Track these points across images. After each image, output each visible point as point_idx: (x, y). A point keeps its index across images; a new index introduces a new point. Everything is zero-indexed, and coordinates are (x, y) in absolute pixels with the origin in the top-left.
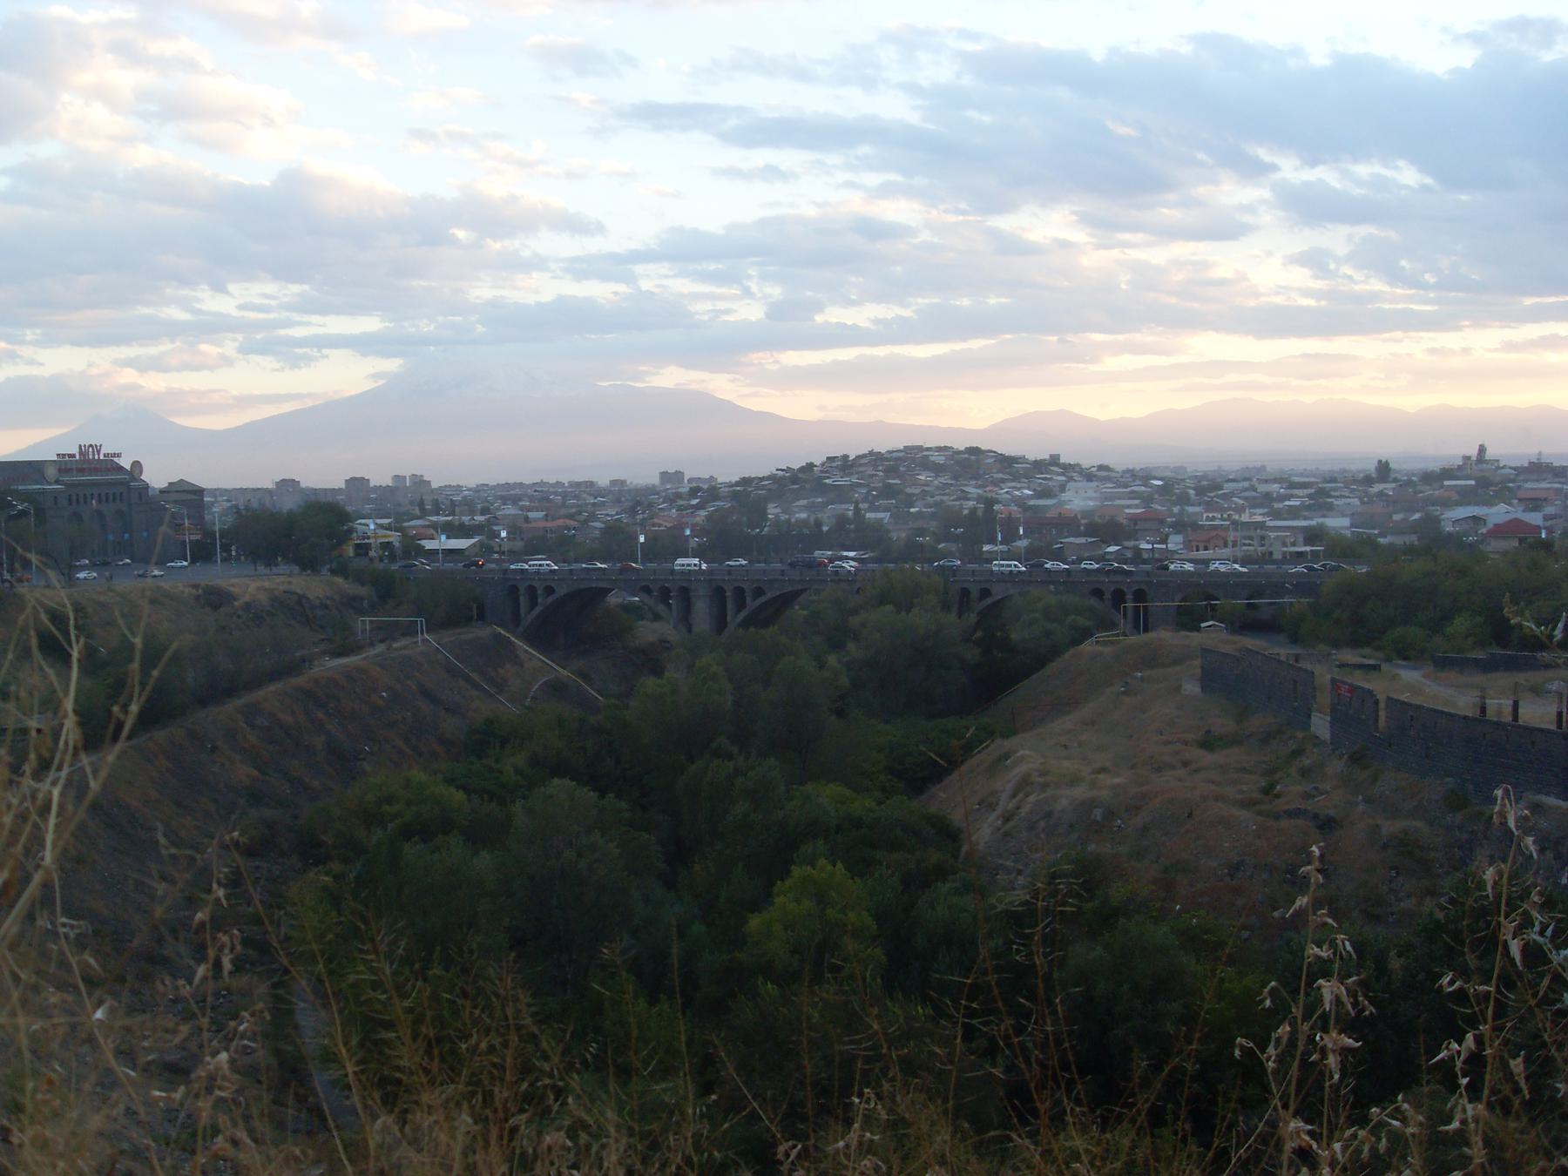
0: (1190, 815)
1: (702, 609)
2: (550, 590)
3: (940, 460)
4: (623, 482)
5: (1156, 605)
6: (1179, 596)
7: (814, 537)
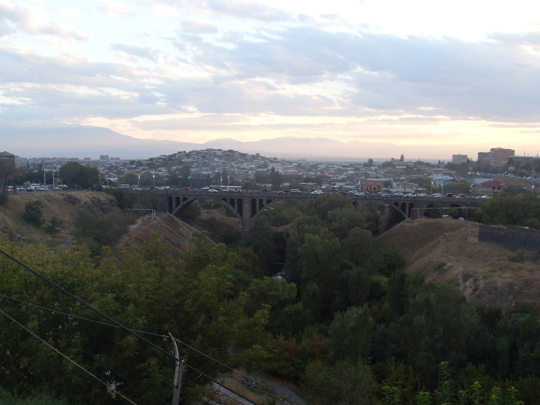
1: (247, 207)
2: (185, 199)
4: (89, 159)
5: (417, 209)
6: (425, 206)
7: (207, 181)
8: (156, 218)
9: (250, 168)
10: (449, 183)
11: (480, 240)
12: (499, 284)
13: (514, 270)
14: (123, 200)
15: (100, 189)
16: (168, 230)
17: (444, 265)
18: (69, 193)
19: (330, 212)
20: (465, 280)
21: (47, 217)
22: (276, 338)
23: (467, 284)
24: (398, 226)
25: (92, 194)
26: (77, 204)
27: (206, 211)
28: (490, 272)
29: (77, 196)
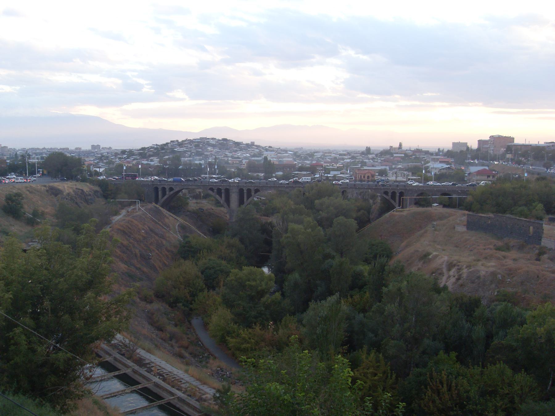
0: (538, 277)
1: (234, 198)
2: (171, 189)
3: (214, 143)
4: (80, 149)
5: (407, 198)
6: (416, 195)
8: (140, 209)
9: (244, 156)
10: (445, 171)
11: (468, 228)
12: (483, 273)
13: (498, 259)
14: (107, 191)
15: (84, 180)
16: (153, 221)
17: (428, 254)
18: (51, 184)
19: (317, 202)
20: (449, 270)
21: (27, 210)
22: (253, 328)
23: (451, 273)
24: (387, 215)
25: (76, 185)
26: (59, 195)
27: (195, 201)
28: (475, 260)
29: (60, 188)
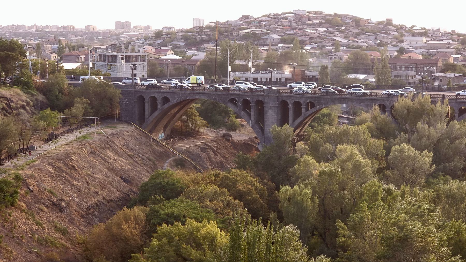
1: (271, 115)
2: (166, 100)
